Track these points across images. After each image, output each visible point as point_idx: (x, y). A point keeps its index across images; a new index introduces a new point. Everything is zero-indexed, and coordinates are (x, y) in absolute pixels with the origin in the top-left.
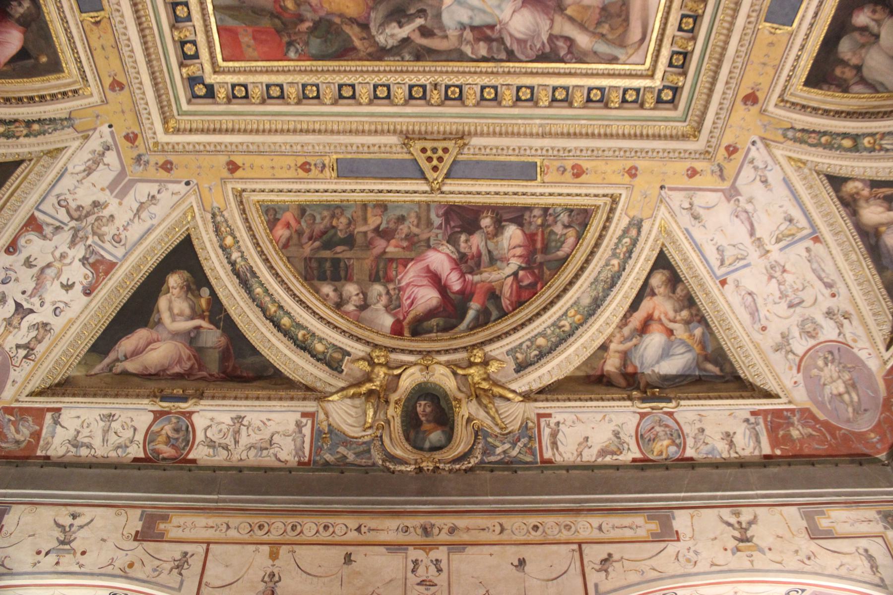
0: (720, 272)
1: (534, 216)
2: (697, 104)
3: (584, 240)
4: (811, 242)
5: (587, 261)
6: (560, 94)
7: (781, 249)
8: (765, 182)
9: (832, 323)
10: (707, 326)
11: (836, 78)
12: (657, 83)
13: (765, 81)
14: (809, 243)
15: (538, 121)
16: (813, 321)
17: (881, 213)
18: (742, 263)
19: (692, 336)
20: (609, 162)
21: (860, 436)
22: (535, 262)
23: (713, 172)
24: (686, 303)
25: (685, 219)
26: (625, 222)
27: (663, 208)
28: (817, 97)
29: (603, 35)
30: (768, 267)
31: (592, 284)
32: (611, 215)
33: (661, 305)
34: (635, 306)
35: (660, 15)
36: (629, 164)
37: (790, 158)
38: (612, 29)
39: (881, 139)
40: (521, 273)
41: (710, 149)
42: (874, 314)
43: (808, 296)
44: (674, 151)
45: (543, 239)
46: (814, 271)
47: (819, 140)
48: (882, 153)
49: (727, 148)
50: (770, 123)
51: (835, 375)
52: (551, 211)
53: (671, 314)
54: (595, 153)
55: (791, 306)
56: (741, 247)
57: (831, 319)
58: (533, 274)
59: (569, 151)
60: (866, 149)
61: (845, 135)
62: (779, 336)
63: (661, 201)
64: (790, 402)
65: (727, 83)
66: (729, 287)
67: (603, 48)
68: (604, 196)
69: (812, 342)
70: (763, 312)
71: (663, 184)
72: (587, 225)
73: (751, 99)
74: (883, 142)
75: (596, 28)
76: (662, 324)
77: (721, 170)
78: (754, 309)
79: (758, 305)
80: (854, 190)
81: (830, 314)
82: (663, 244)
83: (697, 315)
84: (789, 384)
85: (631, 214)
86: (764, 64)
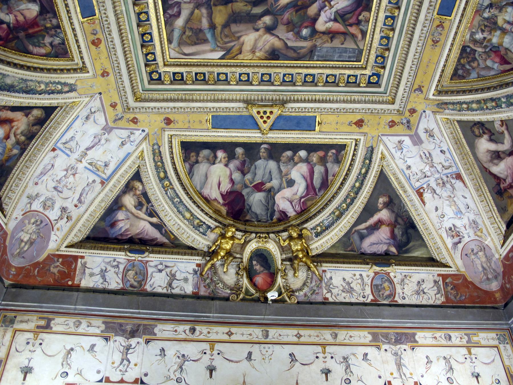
0: (59, 145)
1: (51, 21)
2: (156, 95)
3: (47, 60)
4: (100, 181)
5: (35, 69)
6: (143, 17)
7: (86, 167)
8: (123, 144)
9: (59, 213)
10: (21, 154)
11: (189, 154)
12: (162, 69)
13: (180, 125)
14: (98, 180)
15: (124, 9)
16: (53, 203)
17: (132, 205)
18: (69, 152)
19: (11, 150)
20: (108, 58)
21: (10, 266)
22: (17, 33)
23: (117, 115)
24: (29, 136)
25: (85, 113)
26: (71, 81)
27: (87, 99)
28: (177, 149)
29: (184, 33)
30: (72, 166)
31: (22, 79)
32: (72, 71)
33: (21, 122)
34: (14, 109)
35: (202, 61)
36: (110, 71)
37: (143, 151)
38: (189, 37)
39: (170, 189)
40: (5, 26)
41: (131, 110)
42: (79, 230)
43: (66, 193)
44: (125, 92)
45: (37, 32)
46: (84, 189)
47: (158, 162)
48: (164, 192)
49: (135, 118)
50: (158, 135)
51: (30, 231)
52: (59, 31)
53: (19, 131)
54: (113, 50)
55: (55, 188)
56: (78, 147)
57: (61, 211)
58: (8, 34)
59: (110, 34)
60: (163, 184)
61: (165, 172)
62: (36, 193)
63: (91, 97)
64: (6, 224)
65: (174, 108)
66: (52, 154)
67: (176, 34)
68: (83, 63)
69: (41, 210)
70: (45, 178)
71: (103, 93)
72: (57, 57)
73: (168, 121)
74: (170, 190)
75: (188, 28)
76: (10, 130)
77: (120, 119)
78: (45, 172)
79: (48, 173)
80: (137, 187)
81: (64, 209)
82: (62, 108)
83: (25, 145)
84: (14, 216)
85: (77, 83)
86: (189, 122)
